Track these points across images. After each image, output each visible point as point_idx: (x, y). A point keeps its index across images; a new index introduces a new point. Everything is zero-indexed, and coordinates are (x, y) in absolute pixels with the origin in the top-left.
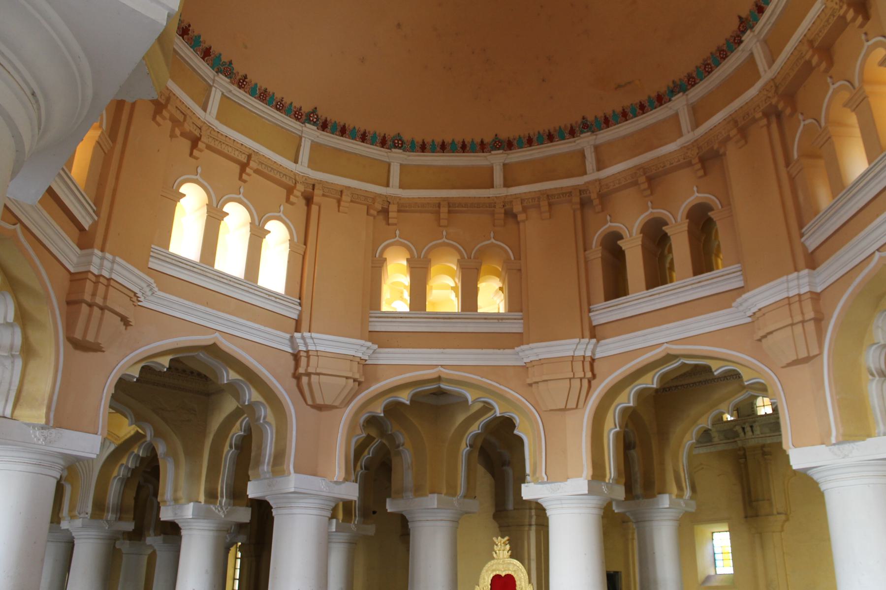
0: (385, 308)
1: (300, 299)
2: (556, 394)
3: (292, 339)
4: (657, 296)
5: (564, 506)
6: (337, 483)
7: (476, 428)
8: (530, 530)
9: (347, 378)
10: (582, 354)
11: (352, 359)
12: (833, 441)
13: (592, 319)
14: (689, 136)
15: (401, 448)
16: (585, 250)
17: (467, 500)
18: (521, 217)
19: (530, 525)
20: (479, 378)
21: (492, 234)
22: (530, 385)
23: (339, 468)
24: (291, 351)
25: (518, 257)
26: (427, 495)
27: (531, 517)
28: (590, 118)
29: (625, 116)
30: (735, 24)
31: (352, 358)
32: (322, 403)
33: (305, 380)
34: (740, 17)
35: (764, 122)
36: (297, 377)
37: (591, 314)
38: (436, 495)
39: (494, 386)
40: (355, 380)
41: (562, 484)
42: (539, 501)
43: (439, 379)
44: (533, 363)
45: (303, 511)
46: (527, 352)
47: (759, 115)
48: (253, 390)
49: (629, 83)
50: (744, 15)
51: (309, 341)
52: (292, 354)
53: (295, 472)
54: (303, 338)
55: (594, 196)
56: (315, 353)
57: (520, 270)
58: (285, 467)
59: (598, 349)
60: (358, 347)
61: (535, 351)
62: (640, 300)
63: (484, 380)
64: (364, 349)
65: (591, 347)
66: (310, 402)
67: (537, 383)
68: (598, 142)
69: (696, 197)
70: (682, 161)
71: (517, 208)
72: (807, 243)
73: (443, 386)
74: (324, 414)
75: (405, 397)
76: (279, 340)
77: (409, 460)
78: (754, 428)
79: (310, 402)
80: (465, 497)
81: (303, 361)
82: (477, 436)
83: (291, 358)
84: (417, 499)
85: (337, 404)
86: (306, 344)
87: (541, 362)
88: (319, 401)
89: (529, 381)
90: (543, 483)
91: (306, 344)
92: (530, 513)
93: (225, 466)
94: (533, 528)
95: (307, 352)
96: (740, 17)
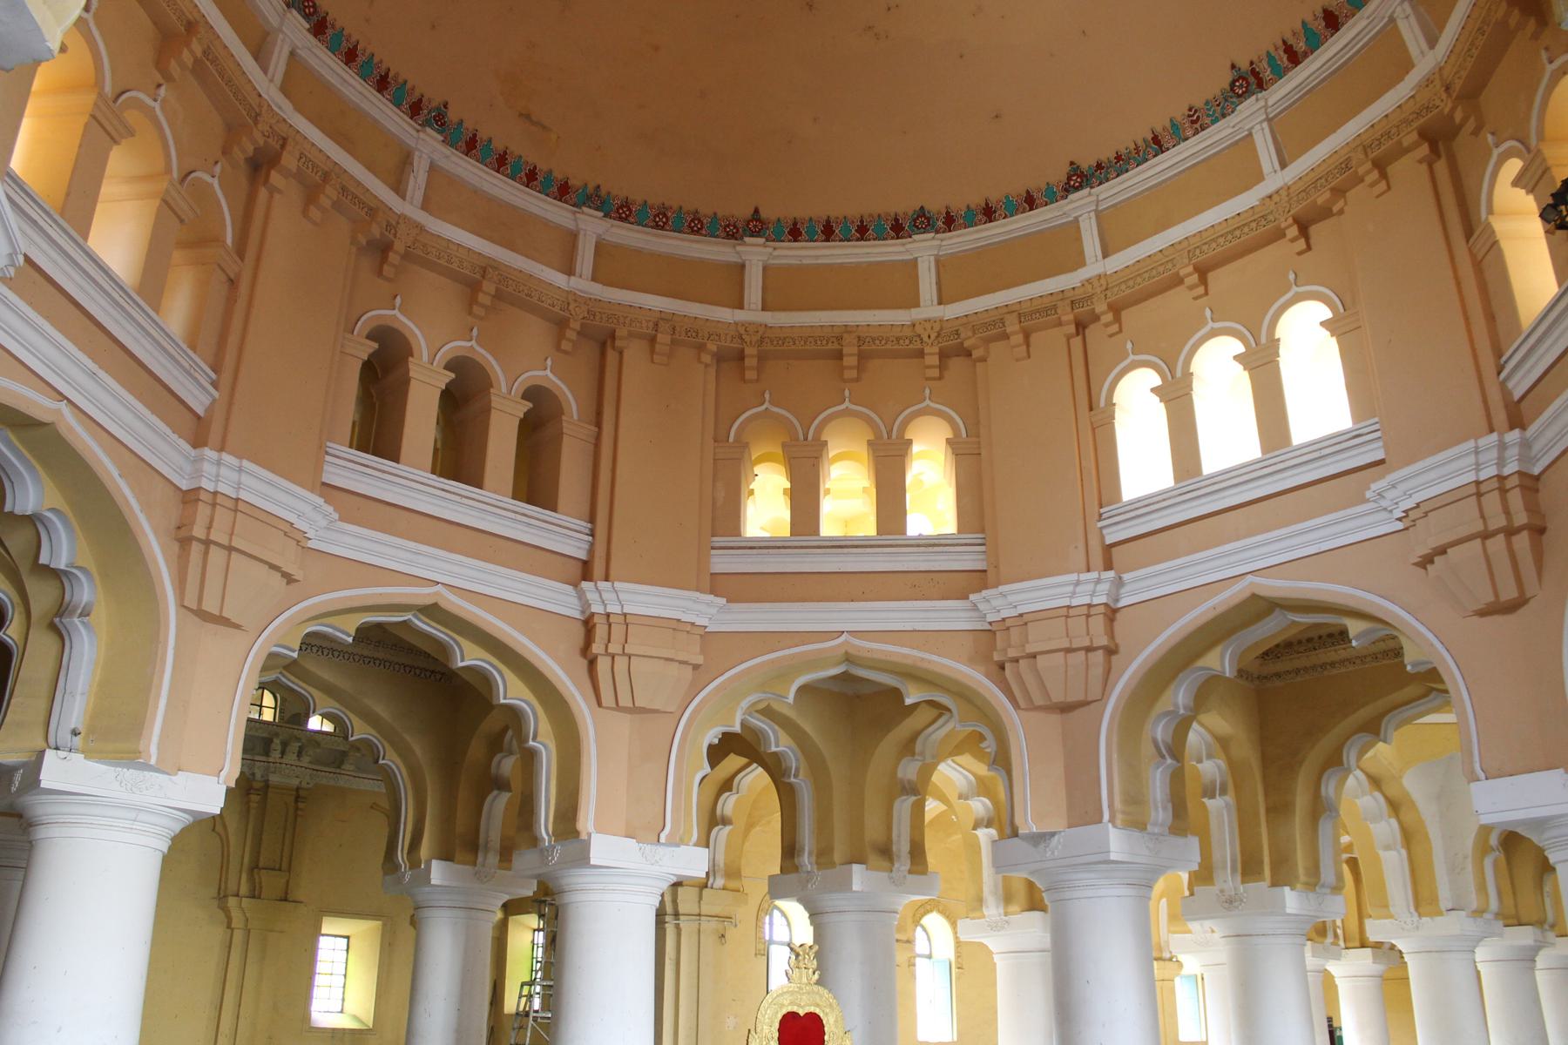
4: (457, 498)
5: (137, 826)
12: (663, 840)
14: (582, 284)
18: (276, 178)
20: (115, 473)
28: (453, 115)
29: (501, 162)
30: (742, 212)
34: (756, 211)
35: (707, 358)
37: (328, 458)
39: (131, 509)
47: (712, 347)
49: (544, 127)
50: (764, 214)
55: (399, 246)
57: (233, 283)
62: (411, 483)
68: (443, 163)
69: (546, 376)
70: (557, 309)
71: (289, 160)
72: (714, 560)
90: (147, 767)
96: (756, 211)
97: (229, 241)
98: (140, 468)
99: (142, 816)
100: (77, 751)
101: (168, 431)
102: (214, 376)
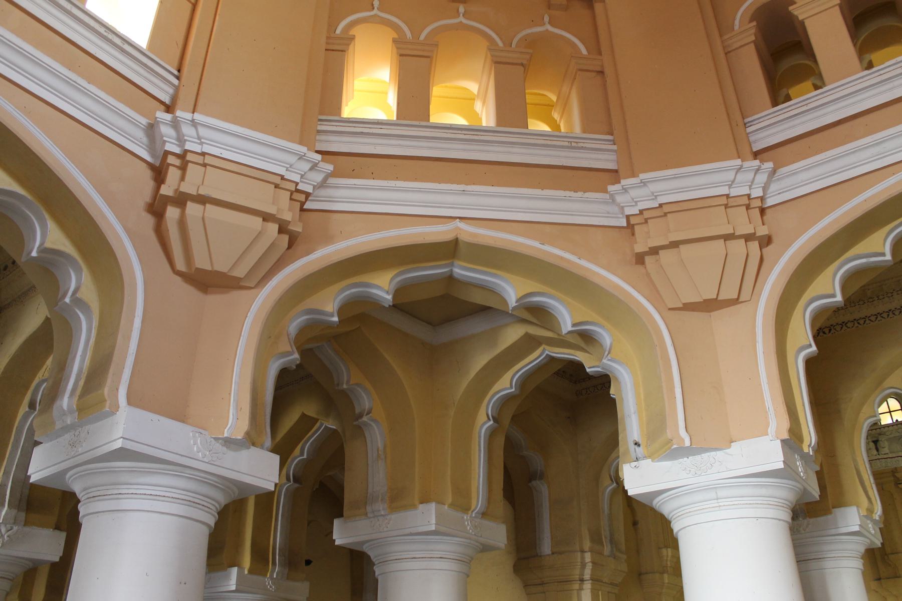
0: (348, 112)
1: (179, 71)
2: (699, 271)
3: (151, 129)
6: (229, 443)
7: (506, 384)
8: (581, 589)
9: (267, 217)
10: (745, 191)
11: (278, 183)
13: (752, 138)
15: (365, 419)
16: (721, 36)
17: (486, 523)
19: (582, 580)
20: (536, 244)
21: (546, 19)
22: (640, 259)
23: (238, 409)
24: (148, 158)
25: (596, 48)
26: (414, 507)
27: (584, 566)
31: (277, 180)
32: (210, 269)
33: (172, 213)
36: (156, 208)
37: (749, 130)
38: (433, 505)
39: (568, 261)
40: (283, 229)
41: (719, 454)
42: (657, 503)
43: (451, 249)
44: (647, 215)
45: (146, 504)
46: (634, 193)
48: (51, 225)
51: (187, 130)
52: (151, 166)
53: (130, 402)
54: (175, 124)
56: (199, 159)
57: (601, 73)
58: (106, 390)
59: (773, 187)
60: (292, 159)
61: (653, 187)
63: (547, 248)
64: (306, 166)
65: (762, 178)
66: (181, 266)
67: (654, 251)
73: (460, 271)
74: (215, 300)
75: (383, 286)
76: (125, 127)
77: (380, 445)
78: (881, 444)
79: (181, 266)
80: (484, 515)
81: (173, 175)
82: (507, 400)
83: (148, 174)
84: (394, 516)
85: (240, 272)
86: (181, 140)
87: (663, 211)
88: (201, 262)
89: (640, 248)
91: (181, 140)
92: (583, 558)
93: (17, 440)
94: (588, 586)
95: (182, 156)
97: (584, 51)
98: (565, 231)
99: (721, 493)
100: (645, 458)
101: (572, 194)
102: (610, 137)
